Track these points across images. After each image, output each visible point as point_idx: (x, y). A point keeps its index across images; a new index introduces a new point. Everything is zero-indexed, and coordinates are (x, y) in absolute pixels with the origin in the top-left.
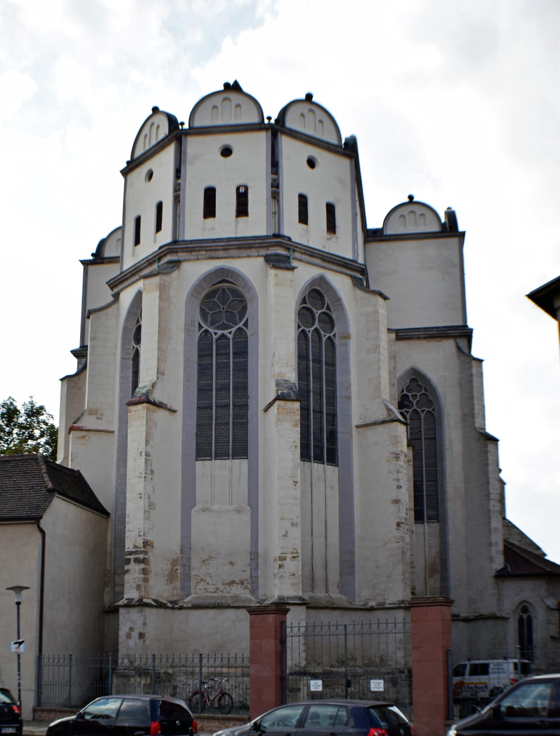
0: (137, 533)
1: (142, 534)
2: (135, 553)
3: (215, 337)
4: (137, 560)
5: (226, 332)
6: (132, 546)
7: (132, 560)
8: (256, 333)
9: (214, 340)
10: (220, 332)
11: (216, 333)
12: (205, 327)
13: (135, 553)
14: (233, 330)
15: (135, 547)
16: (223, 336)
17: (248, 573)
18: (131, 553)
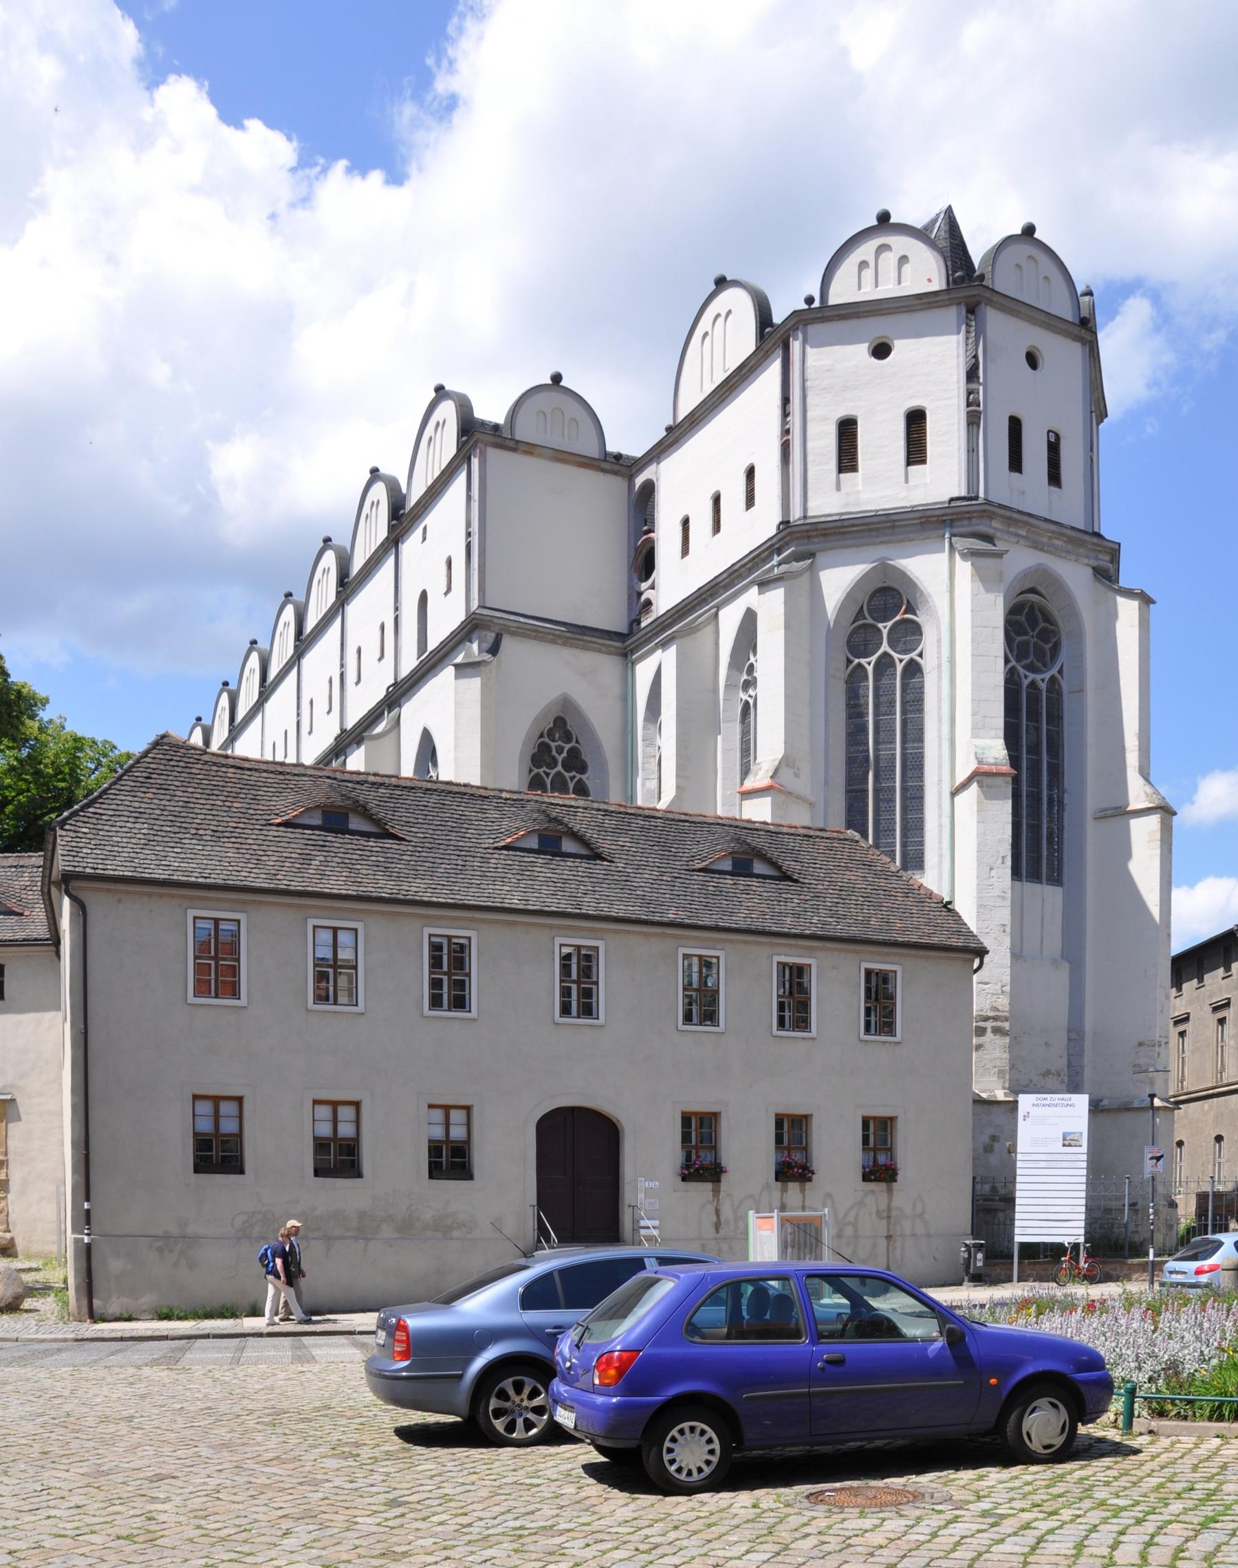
0: (998, 987)
1: (1008, 988)
2: (995, 1018)
3: (1026, 683)
4: (996, 1031)
5: (1038, 677)
6: (988, 1007)
7: (989, 1030)
8: (1081, 690)
9: (1025, 687)
10: (1031, 676)
11: (1027, 678)
12: (1013, 663)
13: (995, 1018)
14: (1047, 676)
15: (995, 1009)
16: (1033, 684)
17: (1065, 1060)
18: (986, 1019)
